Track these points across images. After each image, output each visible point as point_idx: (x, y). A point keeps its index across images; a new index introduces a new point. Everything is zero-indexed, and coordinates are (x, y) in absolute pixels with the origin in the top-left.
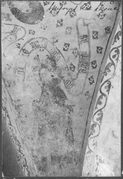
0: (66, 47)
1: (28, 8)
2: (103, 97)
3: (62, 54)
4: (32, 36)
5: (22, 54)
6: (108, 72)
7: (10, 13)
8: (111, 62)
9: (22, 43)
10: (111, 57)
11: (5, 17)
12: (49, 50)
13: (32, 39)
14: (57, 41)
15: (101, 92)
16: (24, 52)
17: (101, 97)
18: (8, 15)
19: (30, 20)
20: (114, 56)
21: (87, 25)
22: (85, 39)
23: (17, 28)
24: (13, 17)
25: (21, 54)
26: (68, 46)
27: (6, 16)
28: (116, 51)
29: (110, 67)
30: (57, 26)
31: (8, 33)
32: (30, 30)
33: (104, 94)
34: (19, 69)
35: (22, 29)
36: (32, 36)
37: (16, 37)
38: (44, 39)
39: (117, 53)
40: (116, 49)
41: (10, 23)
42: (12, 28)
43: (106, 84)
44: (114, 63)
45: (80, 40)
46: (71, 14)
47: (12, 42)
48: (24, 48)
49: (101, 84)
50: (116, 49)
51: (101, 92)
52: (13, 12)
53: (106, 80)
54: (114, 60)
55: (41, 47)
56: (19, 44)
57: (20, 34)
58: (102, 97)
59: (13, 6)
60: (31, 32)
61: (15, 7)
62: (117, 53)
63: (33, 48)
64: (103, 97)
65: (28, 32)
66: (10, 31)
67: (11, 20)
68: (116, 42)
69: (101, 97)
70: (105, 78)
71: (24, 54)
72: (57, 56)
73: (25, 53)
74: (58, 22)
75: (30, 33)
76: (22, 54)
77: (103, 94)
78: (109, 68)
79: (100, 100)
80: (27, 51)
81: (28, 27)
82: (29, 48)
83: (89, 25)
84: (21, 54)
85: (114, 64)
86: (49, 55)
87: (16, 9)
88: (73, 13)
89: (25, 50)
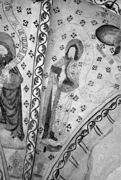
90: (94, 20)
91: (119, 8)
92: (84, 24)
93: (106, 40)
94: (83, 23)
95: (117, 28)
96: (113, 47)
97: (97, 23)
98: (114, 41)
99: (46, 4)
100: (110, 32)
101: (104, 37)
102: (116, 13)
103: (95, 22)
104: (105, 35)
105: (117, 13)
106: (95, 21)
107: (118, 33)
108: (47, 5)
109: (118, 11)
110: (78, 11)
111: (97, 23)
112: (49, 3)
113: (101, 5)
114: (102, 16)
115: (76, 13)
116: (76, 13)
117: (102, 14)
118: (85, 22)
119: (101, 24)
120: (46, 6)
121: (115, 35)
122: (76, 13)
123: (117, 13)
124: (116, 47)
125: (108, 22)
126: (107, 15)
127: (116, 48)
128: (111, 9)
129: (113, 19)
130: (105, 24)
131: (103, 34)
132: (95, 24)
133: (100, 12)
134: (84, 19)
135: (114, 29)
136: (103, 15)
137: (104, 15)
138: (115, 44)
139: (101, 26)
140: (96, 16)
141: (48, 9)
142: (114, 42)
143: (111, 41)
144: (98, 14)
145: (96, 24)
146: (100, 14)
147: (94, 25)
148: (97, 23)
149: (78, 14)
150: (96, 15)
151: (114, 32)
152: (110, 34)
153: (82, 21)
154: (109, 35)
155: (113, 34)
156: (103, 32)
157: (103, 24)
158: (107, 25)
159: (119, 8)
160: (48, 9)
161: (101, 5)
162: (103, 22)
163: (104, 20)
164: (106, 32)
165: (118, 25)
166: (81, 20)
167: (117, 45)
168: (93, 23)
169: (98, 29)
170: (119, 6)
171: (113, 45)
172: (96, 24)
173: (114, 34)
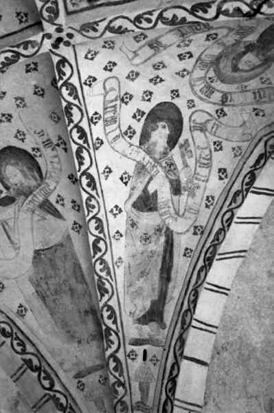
0: (185, 56)
1: (160, 127)
2: (223, 9)
3: (202, 53)
4: (197, 101)
5: (230, 101)
6: (177, 18)
7: (177, 147)
8: (159, 22)
9: (211, 109)
10: (151, 25)
11: (186, 149)
12: (203, 72)
13: (201, 99)
14: (184, 70)
15: (217, 17)
16: (226, 101)
17: (226, 13)
18: (181, 146)
19: (174, 116)
20: (149, 21)
21: (135, 52)
22: (155, 45)
23: (194, 126)
24: (181, 140)
25: (232, 103)
26: (182, 55)
27: (184, 148)
28: (141, 22)
29: (168, 19)
30: (162, 80)
31: (205, 135)
32: (189, 108)
33: (217, 10)
34: (258, 98)
35: (193, 118)
36: (197, 101)
37: (208, 120)
38: (192, 86)
39: (142, 20)
40: (137, 24)
41: (190, 141)
42: (197, 134)
43: (200, 13)
44: (159, 15)
45: (161, 48)
46: (134, 77)
47: (217, 123)
48: (220, 103)
49: (203, 22)
50: (137, 24)
51: (217, 17)
52: (175, 144)
53: (191, 16)
54: (154, 18)
55: (207, 83)
56: (217, 111)
57: (200, 118)
58: (225, 11)
59: (166, 149)
60: (191, 105)
61: (166, 145)
62: (142, 20)
63: (213, 92)
64: (223, 9)
65: (193, 109)
66: (203, 134)
67: (187, 140)
68: (126, 29)
69: (226, 13)
70: (190, 18)
71: (229, 99)
72: (208, 60)
73: (227, 98)
74: (155, 84)
75: (194, 106)
76: (230, 101)
77: (219, 12)
78: (170, 19)
79: (231, 12)
80: (222, 97)
81: (186, 113)
82: (217, 97)
83: (134, 50)
84: (232, 103)
85: (161, 14)
86: (212, 69)
87: (168, 143)
88: (133, 75)
89: (222, 101)
90: (26, 132)
91: (88, 168)
92: (5, 120)
93: (7, 172)
94: (7, 118)
95: (41, 176)
96: (5, 191)
97: (23, 140)
98: (16, 185)
99: (12, 54)
100: (25, 168)
101: (7, 167)
102: (77, 170)
103: (23, 137)
104: (12, 165)
105: (79, 171)
106: (24, 135)
107: (33, 183)
108: (12, 56)
109: (81, 172)
110: (22, 99)
111: (23, 140)
112: (19, 58)
113: (73, 141)
114: (44, 142)
115: (16, 99)
116: (16, 99)
117: (47, 141)
118: (9, 121)
119: (27, 146)
120: (9, 55)
121: (28, 180)
122: (15, 98)
123: (79, 171)
124: (9, 195)
125: (40, 156)
126: (53, 150)
127: (7, 196)
128: (77, 158)
129: (52, 162)
130: (32, 153)
131: (13, 161)
132: (20, 137)
133: (48, 135)
134: (15, 115)
135: (35, 173)
136: (48, 143)
137: (48, 144)
138: (11, 190)
139: (23, 150)
140: (35, 133)
141: (5, 61)
142: (15, 187)
143: (11, 180)
144: (41, 134)
145: (20, 139)
146: (45, 138)
147: (16, 137)
148: (23, 141)
149: (16, 102)
150: (37, 132)
151: (31, 175)
152: (22, 171)
153: (10, 116)
154: (18, 171)
155: (25, 176)
156: (16, 160)
157: (30, 151)
158: (33, 158)
159: (88, 168)
160: (5, 61)
161: (73, 141)
162: (33, 149)
163: (38, 149)
164: (20, 164)
165: (48, 175)
166: (10, 113)
167: (12, 193)
168: (18, 135)
169: (14, 147)
170: (91, 168)
171: (7, 188)
172: (20, 139)
173: (28, 178)
